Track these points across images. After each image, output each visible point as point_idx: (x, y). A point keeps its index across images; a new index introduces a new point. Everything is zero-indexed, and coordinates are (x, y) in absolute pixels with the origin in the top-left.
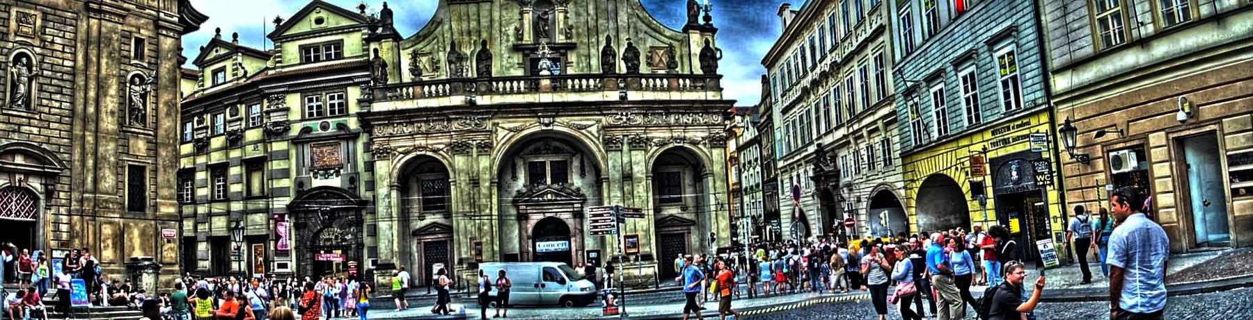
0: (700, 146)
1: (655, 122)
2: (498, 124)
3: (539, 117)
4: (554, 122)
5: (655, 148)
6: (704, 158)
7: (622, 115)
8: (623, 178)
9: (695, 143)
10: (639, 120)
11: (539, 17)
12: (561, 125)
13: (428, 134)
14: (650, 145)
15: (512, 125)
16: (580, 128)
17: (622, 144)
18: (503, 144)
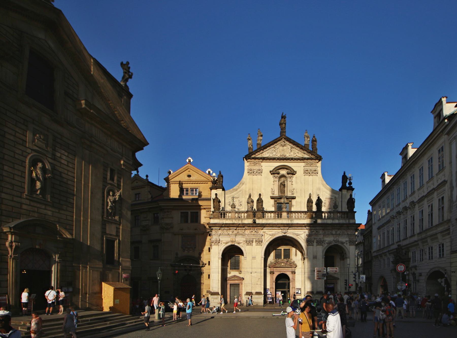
0: (345, 244)
1: (327, 233)
2: (265, 232)
3: (281, 229)
4: (287, 232)
5: (326, 245)
6: (346, 250)
7: (314, 229)
8: (313, 257)
9: (342, 243)
10: (321, 232)
11: (281, 184)
12: (291, 233)
13: (236, 235)
14: (325, 244)
15: (271, 233)
16: (298, 235)
17: (313, 242)
18: (267, 241)
